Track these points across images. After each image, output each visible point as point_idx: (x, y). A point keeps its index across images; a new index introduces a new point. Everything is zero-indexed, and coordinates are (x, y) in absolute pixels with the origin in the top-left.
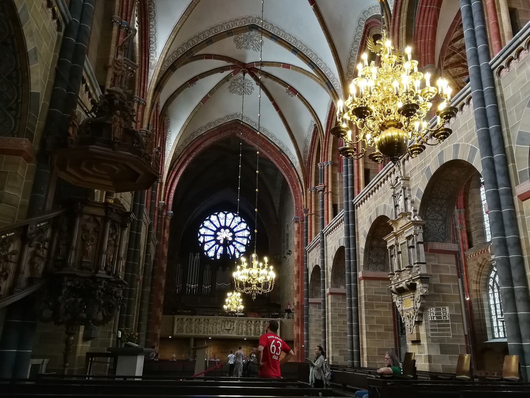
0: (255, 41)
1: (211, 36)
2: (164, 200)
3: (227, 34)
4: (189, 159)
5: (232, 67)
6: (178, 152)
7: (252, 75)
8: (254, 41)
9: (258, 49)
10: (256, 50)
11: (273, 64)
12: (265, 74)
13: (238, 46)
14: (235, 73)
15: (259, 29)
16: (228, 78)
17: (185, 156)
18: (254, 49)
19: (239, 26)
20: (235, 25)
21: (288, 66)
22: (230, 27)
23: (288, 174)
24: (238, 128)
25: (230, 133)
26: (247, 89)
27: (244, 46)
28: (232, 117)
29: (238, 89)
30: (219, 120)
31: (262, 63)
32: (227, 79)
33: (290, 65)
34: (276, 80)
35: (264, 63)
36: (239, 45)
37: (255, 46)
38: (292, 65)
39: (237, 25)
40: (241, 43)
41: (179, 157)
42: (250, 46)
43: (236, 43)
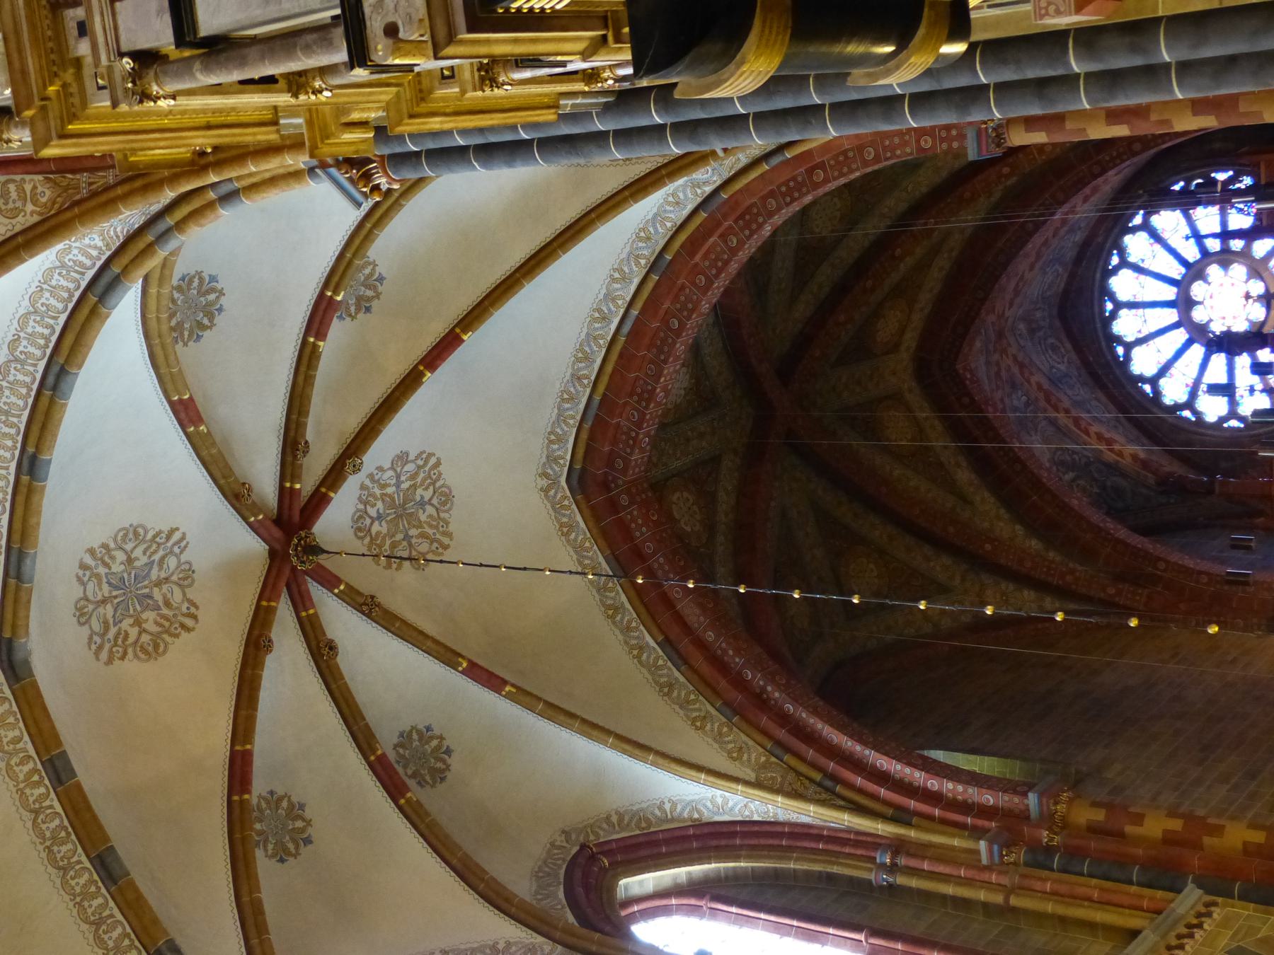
1: (84, 858)
2: (977, 833)
3: (61, 782)
7: (318, 501)
8: (137, 564)
9: (168, 538)
12: (289, 459)
13: (183, 626)
18: (176, 550)
19: (21, 724)
20: (21, 745)
22: (35, 771)
23: (758, 214)
26: (413, 477)
27: (177, 596)
29: (423, 518)
32: (368, 606)
39: (20, 739)
40: (163, 616)
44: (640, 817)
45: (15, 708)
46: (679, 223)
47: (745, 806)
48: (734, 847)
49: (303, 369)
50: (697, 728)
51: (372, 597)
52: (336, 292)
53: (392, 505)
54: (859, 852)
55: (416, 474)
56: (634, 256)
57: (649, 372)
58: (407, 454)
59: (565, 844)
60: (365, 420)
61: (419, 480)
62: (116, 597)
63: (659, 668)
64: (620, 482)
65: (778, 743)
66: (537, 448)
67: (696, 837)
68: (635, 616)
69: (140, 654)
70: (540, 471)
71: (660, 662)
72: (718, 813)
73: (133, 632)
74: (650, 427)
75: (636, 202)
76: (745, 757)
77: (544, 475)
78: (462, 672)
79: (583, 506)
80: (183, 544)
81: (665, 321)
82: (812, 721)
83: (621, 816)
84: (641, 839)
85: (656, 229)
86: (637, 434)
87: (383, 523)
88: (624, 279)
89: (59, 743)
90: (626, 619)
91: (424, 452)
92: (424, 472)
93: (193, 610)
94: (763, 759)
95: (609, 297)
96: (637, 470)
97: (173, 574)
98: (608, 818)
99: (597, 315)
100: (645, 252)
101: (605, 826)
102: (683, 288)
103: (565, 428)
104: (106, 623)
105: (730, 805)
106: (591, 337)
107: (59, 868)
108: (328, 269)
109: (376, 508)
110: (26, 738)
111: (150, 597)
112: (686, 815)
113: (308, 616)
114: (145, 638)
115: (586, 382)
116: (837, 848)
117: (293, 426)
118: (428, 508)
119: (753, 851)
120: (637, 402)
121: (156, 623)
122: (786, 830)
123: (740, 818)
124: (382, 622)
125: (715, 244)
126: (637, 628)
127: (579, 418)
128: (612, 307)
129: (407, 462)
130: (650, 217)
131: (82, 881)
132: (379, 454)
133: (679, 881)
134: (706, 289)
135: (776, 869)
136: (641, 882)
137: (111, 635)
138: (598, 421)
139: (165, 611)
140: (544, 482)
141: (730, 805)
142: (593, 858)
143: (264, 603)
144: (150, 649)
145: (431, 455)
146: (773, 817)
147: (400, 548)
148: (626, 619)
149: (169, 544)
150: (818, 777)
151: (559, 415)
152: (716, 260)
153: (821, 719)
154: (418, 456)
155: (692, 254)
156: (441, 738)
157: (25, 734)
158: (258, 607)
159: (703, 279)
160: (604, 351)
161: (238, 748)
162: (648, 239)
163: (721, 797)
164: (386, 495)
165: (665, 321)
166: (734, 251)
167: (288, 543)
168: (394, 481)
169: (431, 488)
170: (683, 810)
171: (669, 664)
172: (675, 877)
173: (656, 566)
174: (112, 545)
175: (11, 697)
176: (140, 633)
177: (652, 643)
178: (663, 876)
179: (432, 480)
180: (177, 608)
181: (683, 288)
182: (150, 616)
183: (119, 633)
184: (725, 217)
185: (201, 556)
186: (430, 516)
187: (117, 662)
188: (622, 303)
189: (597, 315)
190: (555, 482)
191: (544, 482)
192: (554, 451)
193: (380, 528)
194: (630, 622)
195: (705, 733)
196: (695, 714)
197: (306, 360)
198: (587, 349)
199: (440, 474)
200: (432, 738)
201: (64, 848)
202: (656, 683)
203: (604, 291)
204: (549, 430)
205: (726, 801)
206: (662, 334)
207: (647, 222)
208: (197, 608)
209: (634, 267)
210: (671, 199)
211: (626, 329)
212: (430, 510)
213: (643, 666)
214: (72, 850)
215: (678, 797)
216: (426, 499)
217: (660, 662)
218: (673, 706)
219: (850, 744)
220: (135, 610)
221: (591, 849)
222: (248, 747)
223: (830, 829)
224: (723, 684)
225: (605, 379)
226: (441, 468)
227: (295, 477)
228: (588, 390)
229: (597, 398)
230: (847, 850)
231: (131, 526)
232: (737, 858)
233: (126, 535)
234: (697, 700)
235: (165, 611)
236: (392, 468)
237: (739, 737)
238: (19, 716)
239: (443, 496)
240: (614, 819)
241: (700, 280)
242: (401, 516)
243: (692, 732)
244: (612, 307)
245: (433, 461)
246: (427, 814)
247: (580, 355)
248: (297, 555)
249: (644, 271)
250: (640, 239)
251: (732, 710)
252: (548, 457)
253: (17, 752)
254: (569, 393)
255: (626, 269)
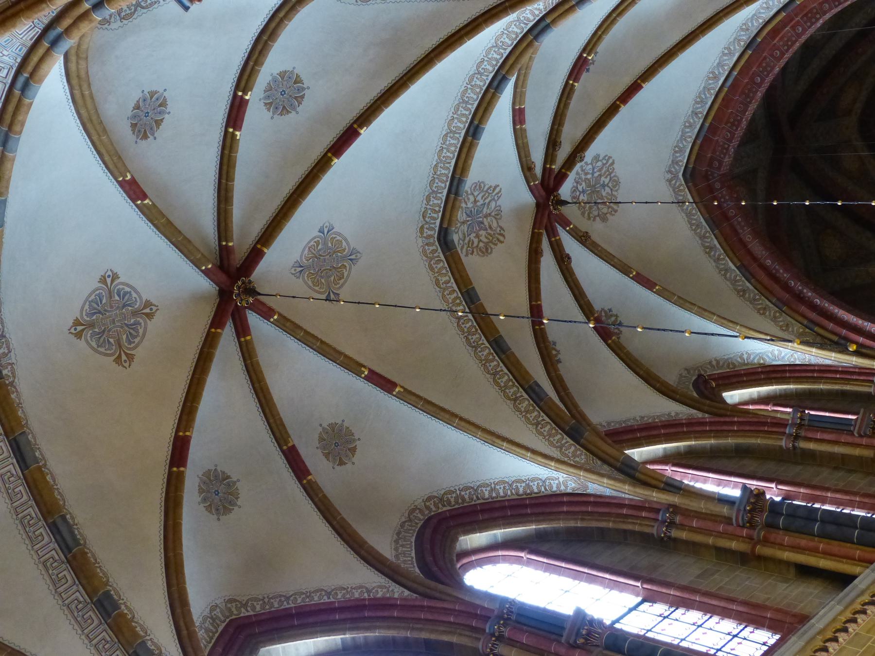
0: (478, 201)
1: (485, 342)
3: (473, 303)
4: (809, 298)
5: (552, 233)
6: (795, 328)
7: (561, 177)
8: (478, 204)
9: (494, 191)
10: (498, 193)
11: (521, 145)
13: (498, 240)
14: (565, 223)
15: (445, 226)
16: (580, 237)
17: (803, 309)
18: (496, 198)
19: (450, 274)
20: (449, 285)
21: (517, 113)
22: (457, 298)
24: (707, 171)
25: (724, 192)
26: (600, 170)
27: (495, 225)
28: (680, 191)
29: (604, 194)
30: (694, 227)
31: (527, 168)
32: (584, 239)
33: (514, 110)
34: (561, 119)
35: (525, 163)
36: (496, 238)
37: (489, 199)
38: (514, 104)
39: (449, 282)
40: (489, 234)
41: (806, 327)
42: (493, 208)
43: (492, 246)
44: (729, 363)
45: (446, 265)
46: (767, 20)
47: (792, 355)
48: (785, 378)
49: (564, 99)
50: (761, 314)
51: (587, 233)
52: (589, 54)
53: (589, 186)
54: (862, 378)
55: (602, 168)
56: (737, 40)
57: (739, 109)
58: (599, 155)
59: (687, 375)
60: (585, 133)
61: (603, 172)
62: (468, 221)
63: (736, 281)
64: (716, 175)
65: (811, 321)
66: (666, 156)
67: (762, 372)
68: (723, 252)
69: (479, 252)
70: (667, 169)
71: (738, 278)
72: (775, 360)
73: (476, 241)
74: (735, 143)
75: (747, 6)
76: (790, 329)
77: (670, 172)
78: (631, 278)
79: (693, 189)
80: (499, 195)
81: (752, 79)
82: (831, 308)
83: (718, 362)
84: (731, 374)
85: (752, 24)
86: (729, 146)
87: (585, 195)
88: (731, 53)
89: (471, 284)
90: (717, 254)
91: (607, 156)
92: (606, 167)
93: (502, 232)
94: (801, 330)
95: (720, 65)
96: (725, 168)
97: (492, 212)
98: (710, 363)
99: (711, 75)
100: (744, 38)
101: (709, 366)
102: (765, 58)
103: (685, 143)
104: (464, 234)
105: (782, 355)
106: (706, 89)
107: (473, 347)
108: (586, 41)
109: (582, 186)
110: (452, 280)
111: (482, 223)
112: (756, 361)
113: (556, 240)
114: (481, 245)
115: (700, 115)
116: (849, 377)
117: (555, 132)
118: (607, 188)
119: (798, 380)
120: (730, 127)
121: (486, 238)
122: (816, 368)
123: (788, 363)
124: (591, 247)
125: (788, 32)
126: (724, 259)
127: (694, 137)
128: (721, 71)
129: (598, 161)
130: (750, 16)
131: (485, 353)
132: (590, 154)
133: (753, 397)
134: (779, 59)
135: (810, 390)
136: (732, 396)
137: (466, 241)
138: (706, 140)
139: (489, 231)
140: (669, 176)
141: (782, 355)
142: (706, 382)
143: (536, 231)
144: (484, 250)
145: (610, 157)
146: (807, 362)
147: (594, 209)
148: (717, 254)
149: (494, 194)
150: (835, 338)
151: (682, 136)
152: (788, 41)
153: (837, 306)
154: (604, 158)
155: (773, 38)
156: (617, 316)
157: (452, 278)
158: (533, 233)
159: (778, 53)
160: (713, 97)
161: (534, 303)
162: (748, 30)
163: (777, 350)
164: (587, 179)
165: (752, 79)
166: (799, 36)
167: (548, 199)
168: (591, 172)
169: (609, 177)
170: (754, 358)
171: (743, 279)
172: (751, 394)
173: (736, 223)
174: (469, 192)
175: (444, 260)
176: (479, 242)
177: (733, 267)
178: (743, 394)
179: (610, 173)
180: (495, 230)
181: (765, 58)
182: (483, 233)
183: (469, 241)
184: (796, 15)
185: (506, 203)
186: (608, 193)
187: (470, 256)
188: (727, 69)
189: (711, 75)
190: (675, 177)
191: (669, 176)
192: (677, 157)
193: (583, 198)
194: (719, 255)
195: (766, 317)
196: (759, 307)
197: (567, 93)
198: (703, 96)
199: (614, 169)
200: (611, 316)
201: (474, 337)
202: (736, 289)
203: (717, 61)
204: (675, 145)
205: (780, 352)
206: (749, 87)
207: (748, 19)
208: (504, 230)
209: (737, 46)
210: (765, 5)
211: (729, 83)
212: (607, 189)
213: (727, 280)
214: (478, 337)
215: (752, 351)
216: (606, 183)
217: (738, 278)
218: (746, 302)
219: (855, 319)
220: (476, 229)
221: (705, 377)
222: (539, 303)
223: (843, 367)
224: (776, 288)
225: (713, 113)
226: (615, 166)
227: (553, 161)
228: (701, 121)
229: (707, 125)
230: (854, 377)
231: (479, 182)
232: (788, 383)
233: (476, 187)
234: (760, 299)
235: (489, 231)
236: (591, 164)
237: (784, 319)
238: (448, 269)
239: (614, 182)
240: (714, 363)
241: (776, 53)
242: (593, 191)
243: (757, 315)
244: (721, 71)
245: (611, 161)
246: (624, 348)
247: (698, 100)
248: (552, 205)
249: (742, 49)
250: (742, 30)
251: (781, 304)
252: (673, 161)
253: (447, 288)
254: (689, 123)
255: (732, 48)
